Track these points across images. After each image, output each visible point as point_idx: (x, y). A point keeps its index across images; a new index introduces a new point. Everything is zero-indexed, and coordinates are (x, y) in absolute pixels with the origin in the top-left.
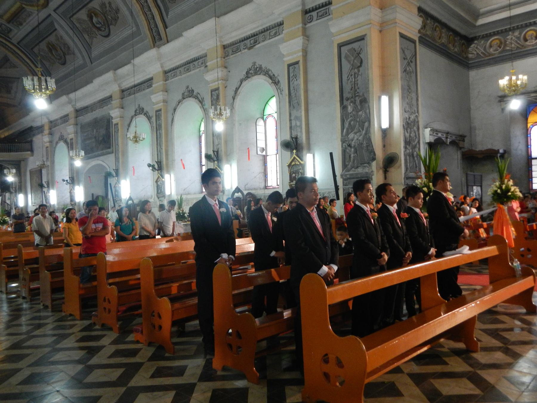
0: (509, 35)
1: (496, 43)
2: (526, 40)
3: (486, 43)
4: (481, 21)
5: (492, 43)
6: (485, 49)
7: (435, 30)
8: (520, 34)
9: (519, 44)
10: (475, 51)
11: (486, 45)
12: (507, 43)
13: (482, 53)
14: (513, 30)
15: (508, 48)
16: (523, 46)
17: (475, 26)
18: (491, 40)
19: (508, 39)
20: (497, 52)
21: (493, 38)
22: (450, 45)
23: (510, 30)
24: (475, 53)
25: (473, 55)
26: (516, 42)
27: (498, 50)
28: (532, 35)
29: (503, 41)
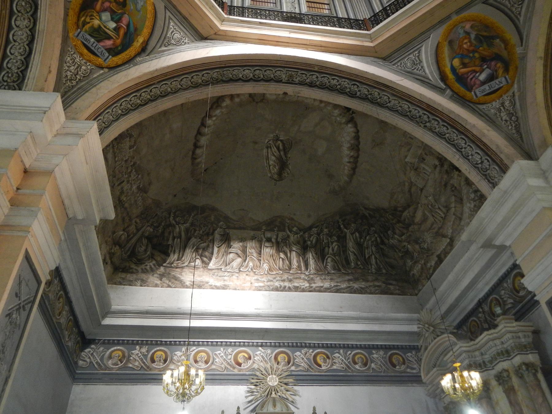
0: (136, 349)
1: (117, 355)
2: (153, 361)
3: (106, 351)
4: (108, 321)
5: (113, 354)
6: (102, 359)
7: (59, 300)
8: (148, 351)
9: (144, 363)
10: (89, 358)
11: (104, 355)
12: (131, 358)
13: (97, 363)
14: (141, 344)
15: (131, 365)
16: (148, 367)
17: (100, 323)
18: (112, 349)
19: (132, 354)
20: (117, 366)
21: (115, 348)
22: (67, 333)
23: (137, 343)
24: (88, 360)
25: (85, 363)
26: (142, 360)
27: (117, 365)
28: (160, 357)
29: (126, 354)
